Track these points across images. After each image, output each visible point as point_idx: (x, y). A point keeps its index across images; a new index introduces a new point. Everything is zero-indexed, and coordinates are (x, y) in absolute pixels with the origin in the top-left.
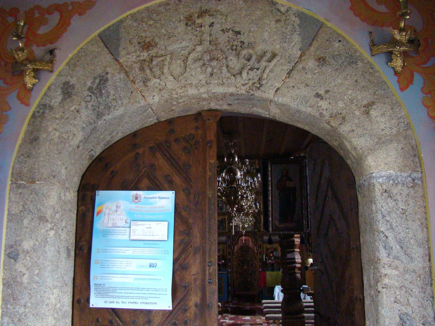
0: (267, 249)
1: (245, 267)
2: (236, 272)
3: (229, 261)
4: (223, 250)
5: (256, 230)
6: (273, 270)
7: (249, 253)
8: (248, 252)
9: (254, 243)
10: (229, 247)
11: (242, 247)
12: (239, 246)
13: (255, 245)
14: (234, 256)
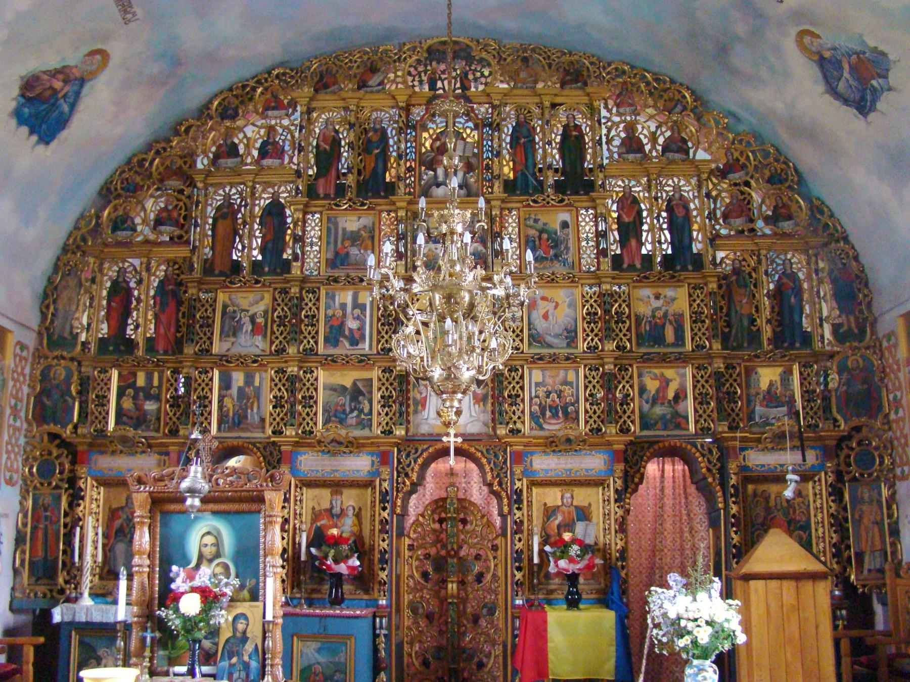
0: (549, 512)
1: (452, 587)
2: (414, 610)
3: (383, 561)
4: (358, 516)
5: (502, 431)
6: (573, 603)
7: (468, 527)
8: (464, 522)
9: (490, 485)
10: (383, 500)
11: (439, 504)
12: (428, 499)
13: (497, 495)
14: (407, 541)
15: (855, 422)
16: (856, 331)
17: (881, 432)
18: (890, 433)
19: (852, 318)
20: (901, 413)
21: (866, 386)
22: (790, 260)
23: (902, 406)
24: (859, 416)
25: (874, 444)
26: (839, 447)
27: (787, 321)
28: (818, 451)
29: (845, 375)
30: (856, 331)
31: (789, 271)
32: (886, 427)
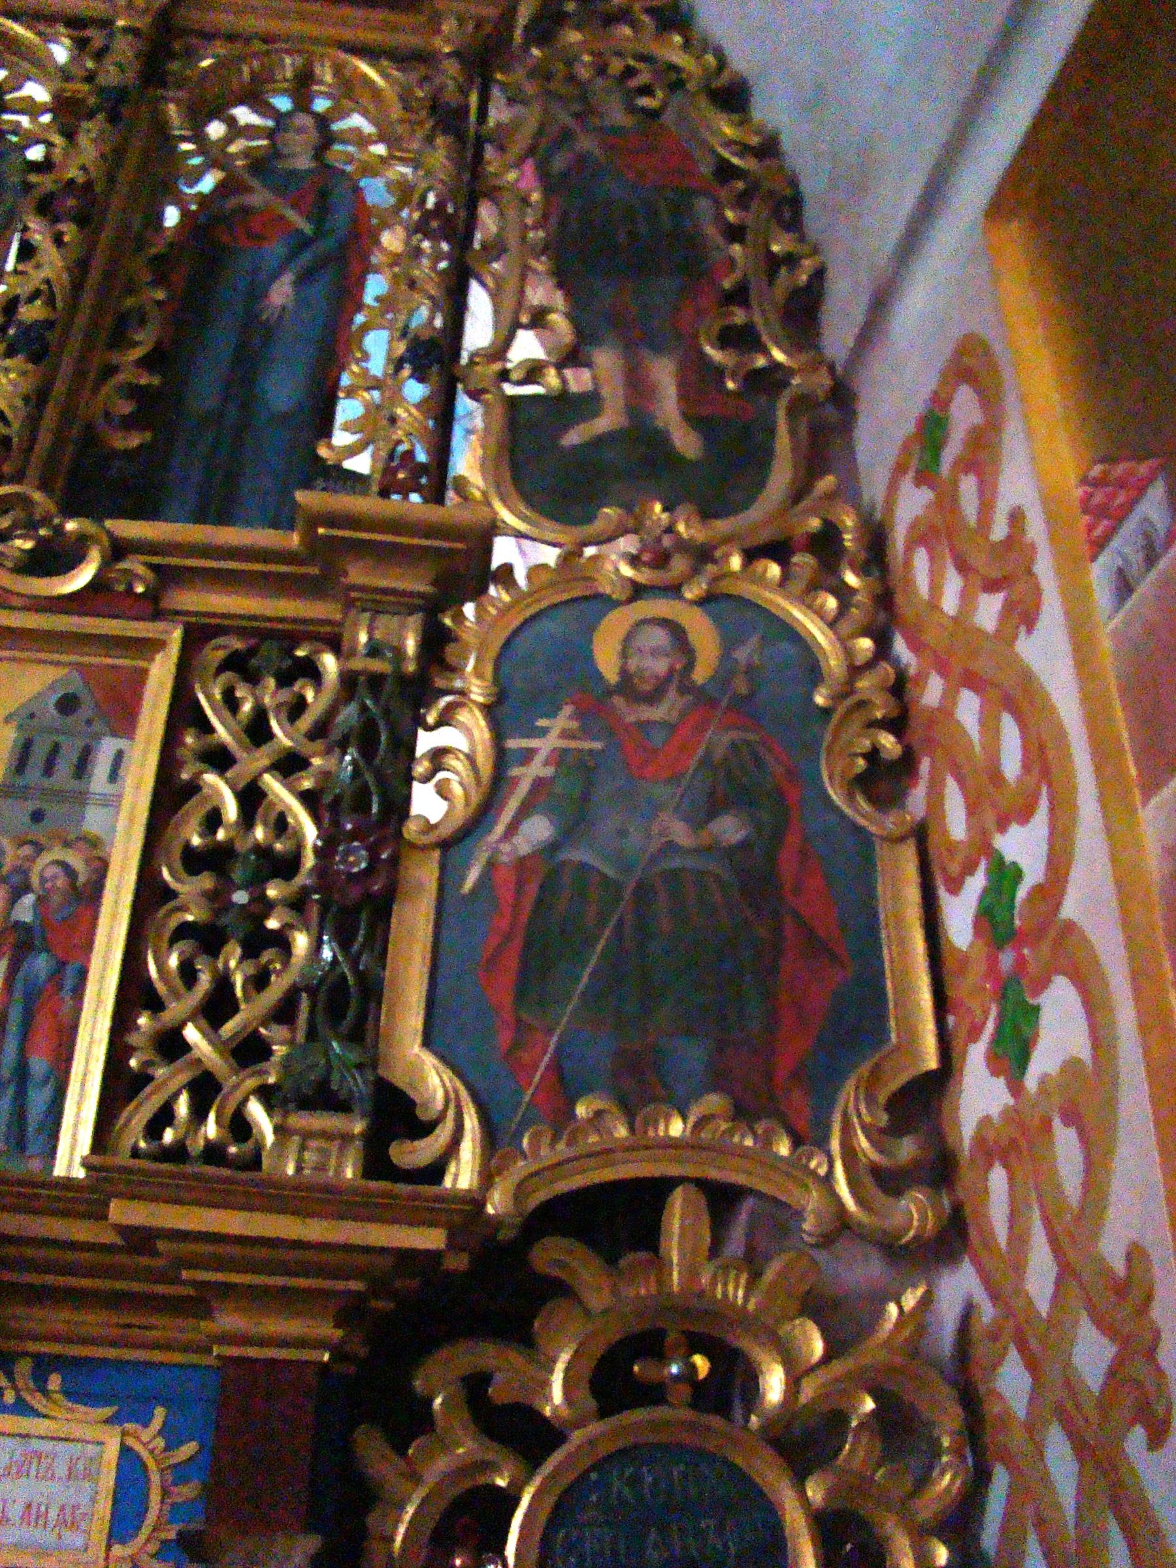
15: (604, 1141)
16: (687, 443)
17: (861, 1270)
18: (959, 1285)
19: (664, 374)
20: (1061, 1029)
21: (730, 829)
22: (323, 121)
23: (1072, 958)
24: (641, 1086)
25: (774, 1385)
26: (372, 1391)
27: (205, 391)
28: (148, 1438)
29: (551, 737)
30: (687, 443)
31: (304, 162)
32: (914, 1211)
